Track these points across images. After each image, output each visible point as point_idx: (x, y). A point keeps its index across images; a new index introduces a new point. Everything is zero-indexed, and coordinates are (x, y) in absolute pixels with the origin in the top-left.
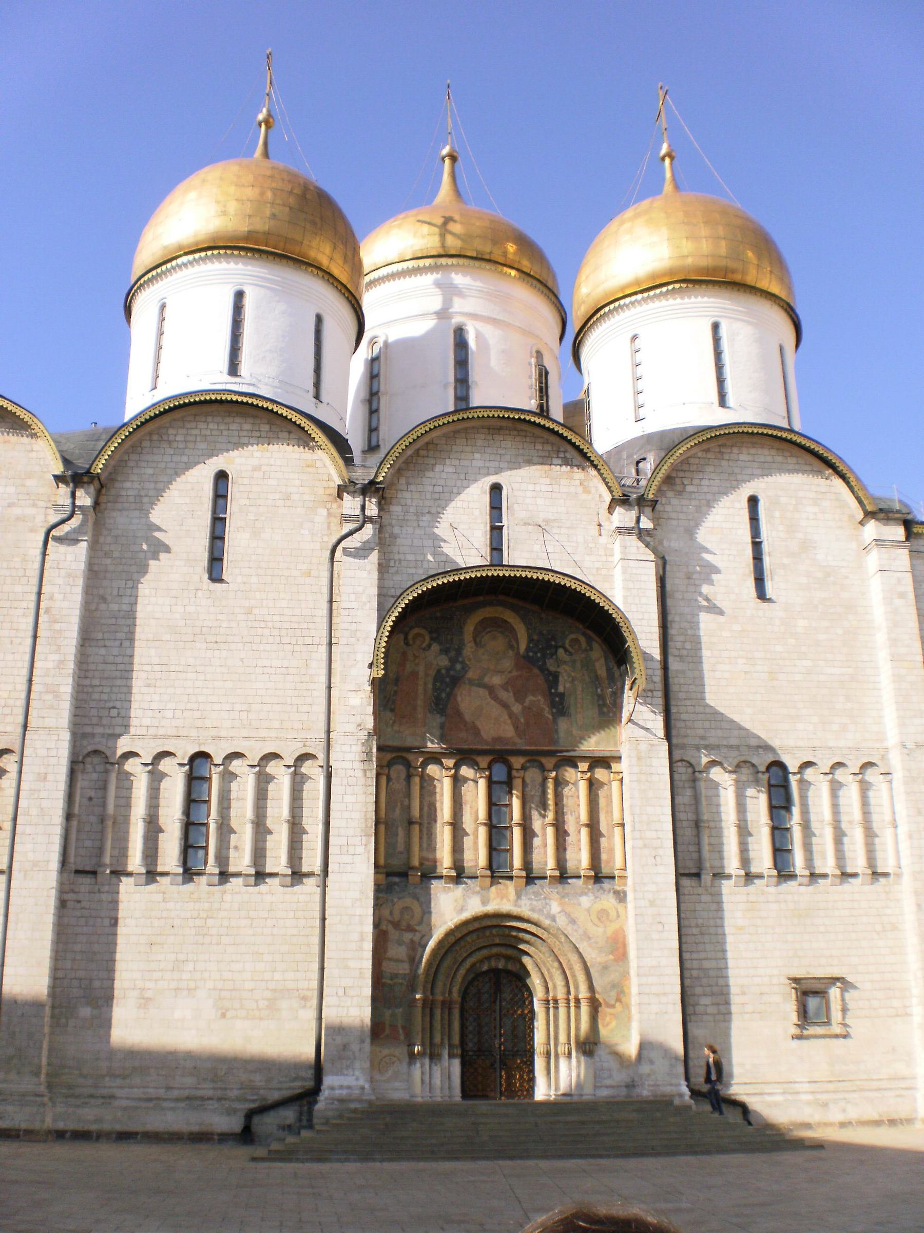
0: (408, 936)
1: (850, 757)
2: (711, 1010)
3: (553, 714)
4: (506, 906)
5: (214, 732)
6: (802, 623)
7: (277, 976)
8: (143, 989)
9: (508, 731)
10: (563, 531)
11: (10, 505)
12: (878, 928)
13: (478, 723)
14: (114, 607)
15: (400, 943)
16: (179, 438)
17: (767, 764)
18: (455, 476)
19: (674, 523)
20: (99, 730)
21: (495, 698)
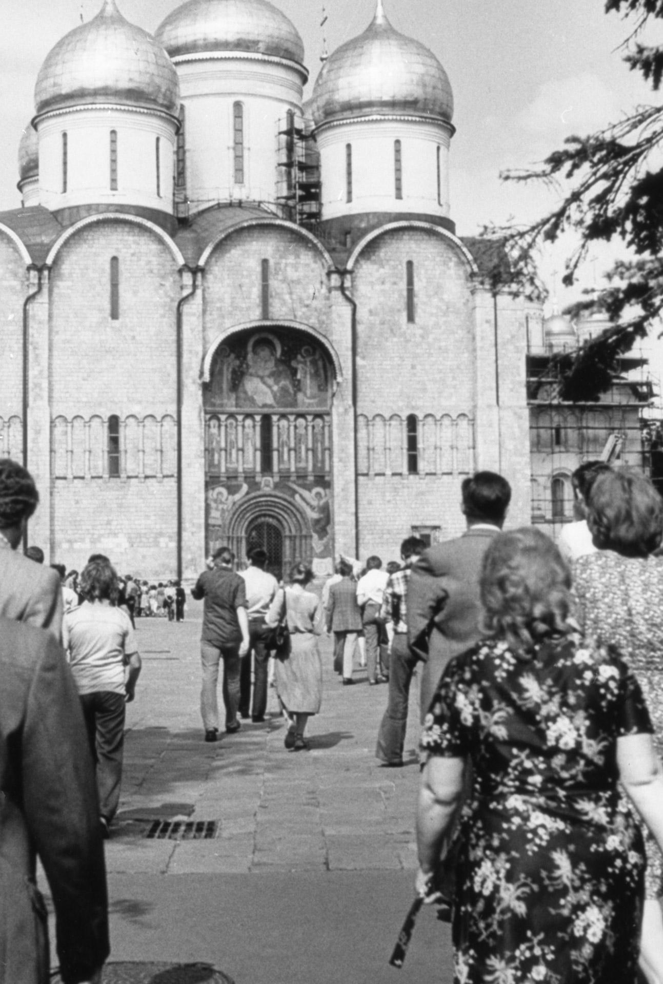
0: (220, 507)
8: (93, 534)
9: (270, 400)
13: (255, 397)
15: (217, 509)
16: (90, 237)
21: (264, 383)
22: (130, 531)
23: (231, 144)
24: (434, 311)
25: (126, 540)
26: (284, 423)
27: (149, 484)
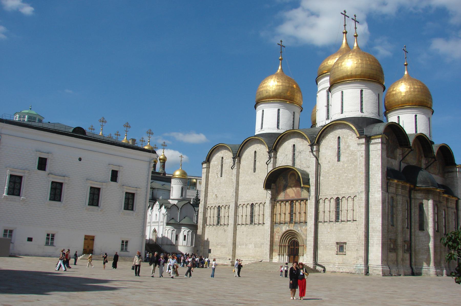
0: (278, 234)
1: (352, 195)
2: (323, 248)
3: (301, 191)
4: (292, 229)
5: (254, 200)
6: (346, 165)
7: (262, 241)
9: (294, 195)
10: (304, 152)
11: (230, 163)
12: (354, 232)
13: (290, 194)
14: (242, 179)
17: (336, 198)
18: (287, 144)
19: (323, 146)
20: (241, 201)
22: (255, 242)
23: (326, 104)
24: (347, 155)
25: (253, 245)
26: (297, 203)
27: (260, 226)
